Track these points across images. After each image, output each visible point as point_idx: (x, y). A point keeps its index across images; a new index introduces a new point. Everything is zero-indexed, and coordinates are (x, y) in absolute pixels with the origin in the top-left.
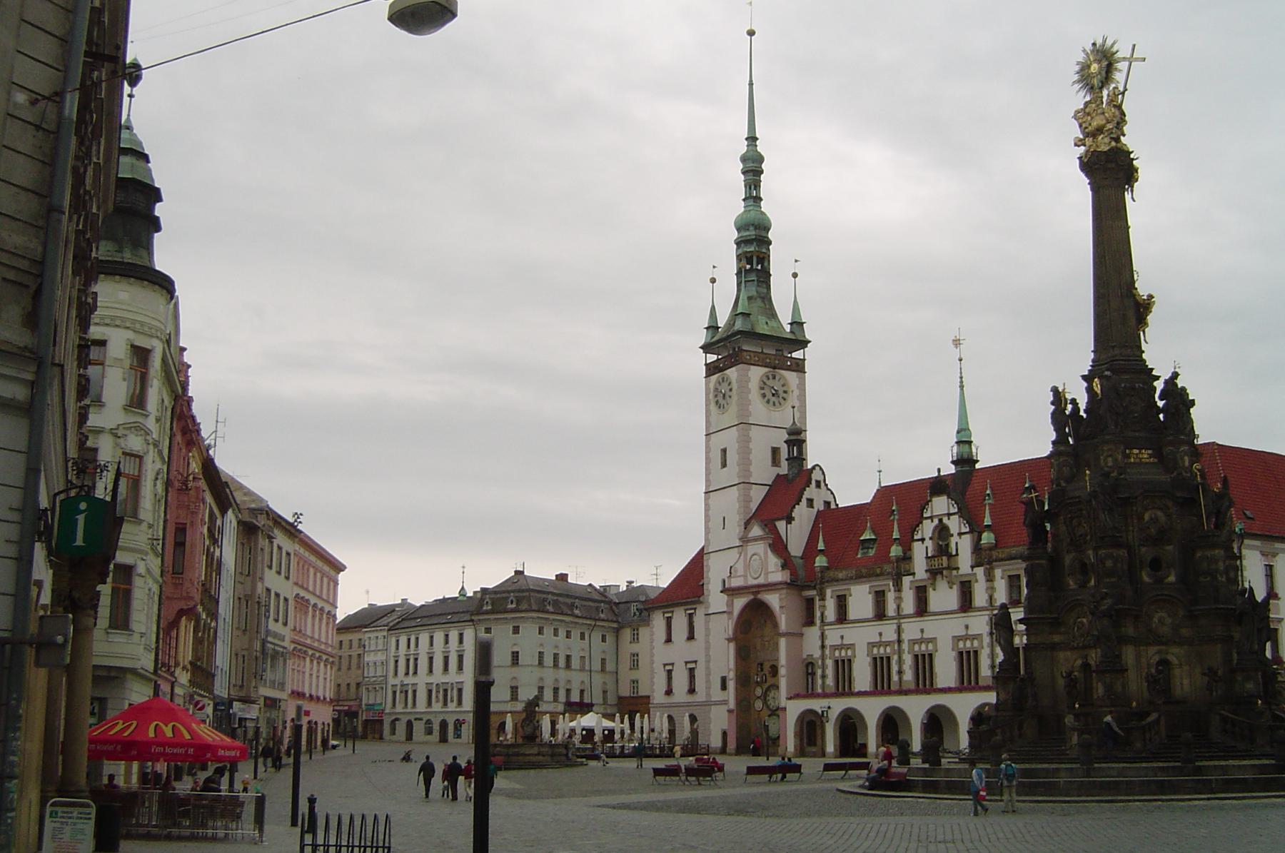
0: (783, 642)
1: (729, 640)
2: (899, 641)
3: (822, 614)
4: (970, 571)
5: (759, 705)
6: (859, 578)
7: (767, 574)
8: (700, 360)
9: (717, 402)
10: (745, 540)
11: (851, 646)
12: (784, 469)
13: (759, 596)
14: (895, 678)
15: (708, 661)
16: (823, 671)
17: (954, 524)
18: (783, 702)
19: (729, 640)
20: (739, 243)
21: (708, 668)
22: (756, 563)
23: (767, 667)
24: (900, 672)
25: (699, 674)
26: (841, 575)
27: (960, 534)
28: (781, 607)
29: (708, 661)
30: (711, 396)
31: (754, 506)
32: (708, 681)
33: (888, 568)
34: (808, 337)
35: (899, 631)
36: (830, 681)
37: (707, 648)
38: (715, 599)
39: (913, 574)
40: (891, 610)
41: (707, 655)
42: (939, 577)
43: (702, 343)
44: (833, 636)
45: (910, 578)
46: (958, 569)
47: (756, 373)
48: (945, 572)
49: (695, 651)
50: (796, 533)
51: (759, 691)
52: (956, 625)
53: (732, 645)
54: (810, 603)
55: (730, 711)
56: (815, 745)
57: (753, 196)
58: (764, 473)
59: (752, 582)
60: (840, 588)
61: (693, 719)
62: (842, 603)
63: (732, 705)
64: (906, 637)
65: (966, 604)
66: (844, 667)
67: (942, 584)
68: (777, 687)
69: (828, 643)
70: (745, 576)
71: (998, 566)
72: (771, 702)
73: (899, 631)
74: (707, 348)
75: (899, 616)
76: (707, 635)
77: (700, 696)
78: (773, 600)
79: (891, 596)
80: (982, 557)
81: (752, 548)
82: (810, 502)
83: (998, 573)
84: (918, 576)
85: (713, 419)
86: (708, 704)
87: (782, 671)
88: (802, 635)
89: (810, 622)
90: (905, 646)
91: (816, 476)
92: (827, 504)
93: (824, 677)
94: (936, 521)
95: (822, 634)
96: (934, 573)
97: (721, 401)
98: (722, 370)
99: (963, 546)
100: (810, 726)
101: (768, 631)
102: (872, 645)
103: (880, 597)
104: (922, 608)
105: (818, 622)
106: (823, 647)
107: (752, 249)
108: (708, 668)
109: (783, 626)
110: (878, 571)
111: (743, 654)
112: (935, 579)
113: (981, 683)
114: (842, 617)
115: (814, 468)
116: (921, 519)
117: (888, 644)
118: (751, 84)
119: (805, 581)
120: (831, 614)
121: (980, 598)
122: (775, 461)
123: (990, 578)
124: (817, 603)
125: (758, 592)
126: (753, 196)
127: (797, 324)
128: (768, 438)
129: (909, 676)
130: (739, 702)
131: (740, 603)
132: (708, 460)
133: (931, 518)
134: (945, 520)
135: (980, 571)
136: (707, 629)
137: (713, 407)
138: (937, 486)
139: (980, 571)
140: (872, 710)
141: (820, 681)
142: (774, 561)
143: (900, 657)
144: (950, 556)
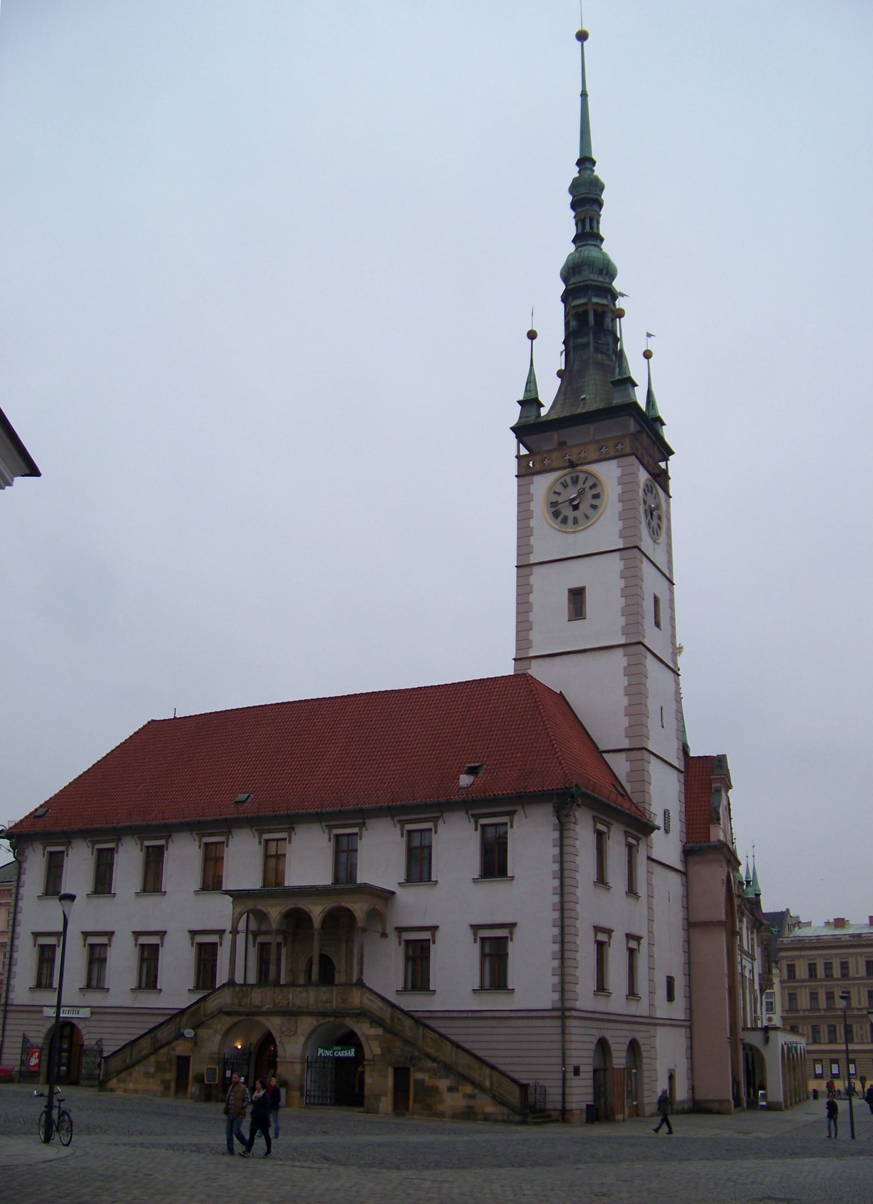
15: (651, 944)
21: (651, 956)
29: (651, 944)
41: (650, 932)
57: (587, 233)
61: (634, 1047)
86: (652, 1022)
108: (651, 956)
118: (584, 95)
126: (587, 233)
136: (649, 884)
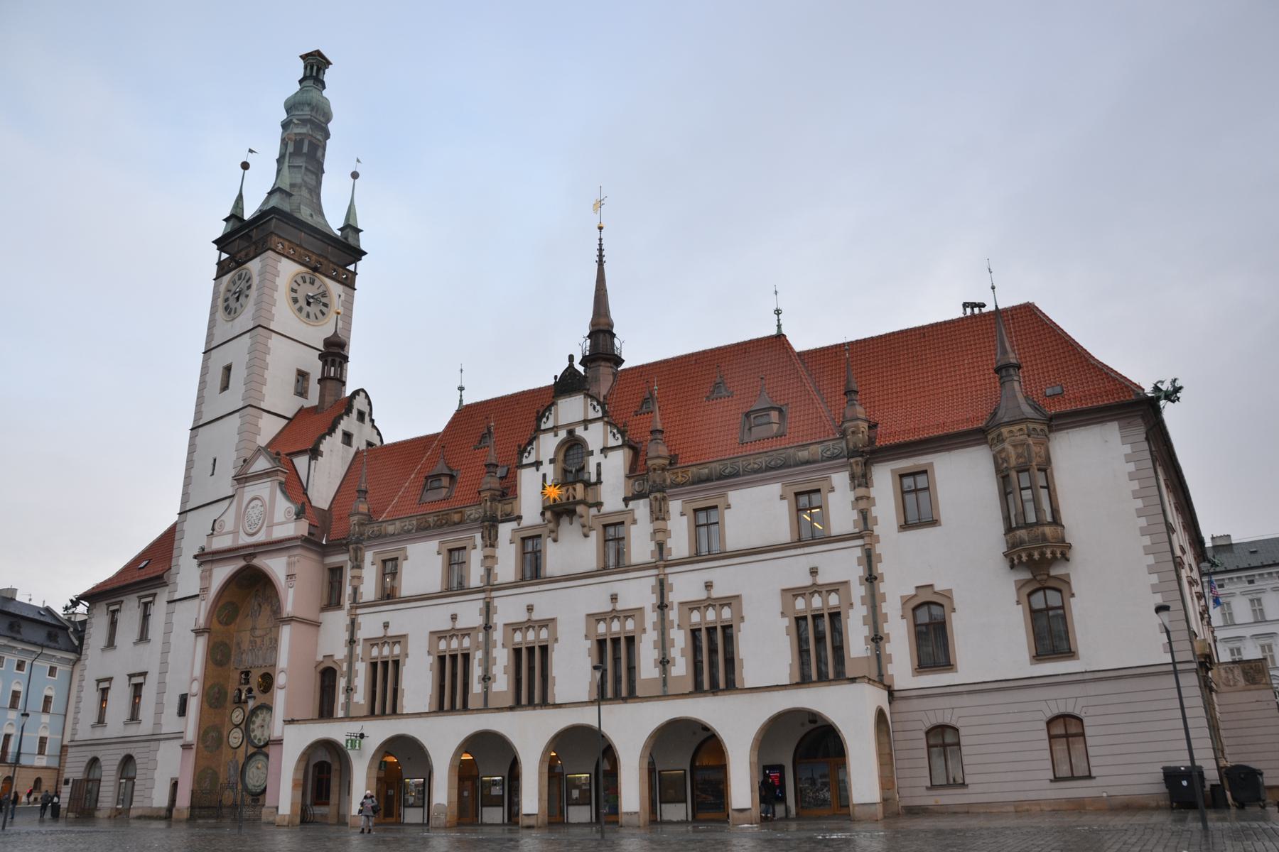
0: (286, 633)
1: (198, 632)
2: (488, 627)
3: (355, 590)
4: (621, 506)
5: (236, 737)
6: (424, 530)
7: (271, 526)
8: (213, 255)
9: (226, 308)
10: (242, 479)
11: (400, 639)
12: (313, 399)
13: (257, 562)
14: (476, 687)
15: (163, 673)
16: (349, 681)
17: (595, 436)
18: (277, 728)
19: (198, 632)
20: (285, 125)
21: (162, 683)
22: (255, 512)
23: (255, 680)
24: (486, 679)
25: (148, 693)
26: (390, 529)
27: (605, 450)
28: (290, 576)
29: (163, 673)
30: (220, 301)
31: (263, 440)
32: (160, 704)
33: (474, 512)
34: (363, 247)
35: (488, 610)
36: (360, 697)
37: (165, 652)
38: (187, 576)
39: (519, 518)
40: (475, 576)
41: (164, 663)
42: (565, 521)
43: (219, 233)
44: (370, 625)
45: (513, 525)
46: (599, 505)
47: (288, 270)
48: (580, 509)
49: (147, 657)
50: (325, 476)
51: (238, 716)
52: (594, 597)
53: (202, 642)
54: (335, 574)
55: (186, 747)
56: (326, 803)
58: (281, 398)
59: (244, 540)
60: (388, 550)
61: (128, 760)
62: (390, 568)
63: (191, 736)
64: (499, 620)
65: (615, 561)
66: (386, 676)
67: (569, 530)
68: (268, 708)
69: (361, 635)
70: (235, 533)
71: (675, 496)
72: (257, 733)
73: (488, 610)
74: (221, 243)
75: (490, 586)
76: (168, 633)
77: (145, 727)
78: (276, 566)
79: (475, 558)
80: (647, 482)
81: (251, 490)
82: (348, 437)
83: (675, 506)
84: (524, 523)
85: (216, 331)
86: (155, 739)
87: (280, 679)
88: (317, 625)
89: (333, 602)
90: (498, 635)
91: (359, 403)
92: (369, 444)
93: (349, 690)
94: (563, 434)
95: (353, 622)
96: (559, 512)
97: (233, 304)
98: (239, 264)
99: (612, 470)
100: (324, 769)
101: (263, 620)
102: (439, 635)
103: (454, 558)
104: (532, 570)
105: (347, 602)
106: (352, 642)
107: (304, 130)
108: (162, 683)
109: (289, 608)
110: (456, 518)
111: (219, 655)
112: (558, 524)
113: (639, 693)
114: (388, 596)
115: (356, 393)
116: (538, 431)
117: (466, 632)
119: (328, 537)
120: (369, 590)
121: (640, 547)
122: (301, 392)
123: (659, 514)
124: (348, 573)
125: (254, 555)
127: (351, 228)
128: (290, 353)
129: (502, 683)
130: (203, 734)
131: (222, 573)
132: (203, 383)
133: (555, 429)
134: (579, 431)
135: (641, 509)
136: (169, 624)
137: (220, 314)
138: (568, 384)
139: (641, 509)
140: (443, 739)
141: (341, 698)
142: (283, 507)
143: (487, 653)
144: (587, 484)
